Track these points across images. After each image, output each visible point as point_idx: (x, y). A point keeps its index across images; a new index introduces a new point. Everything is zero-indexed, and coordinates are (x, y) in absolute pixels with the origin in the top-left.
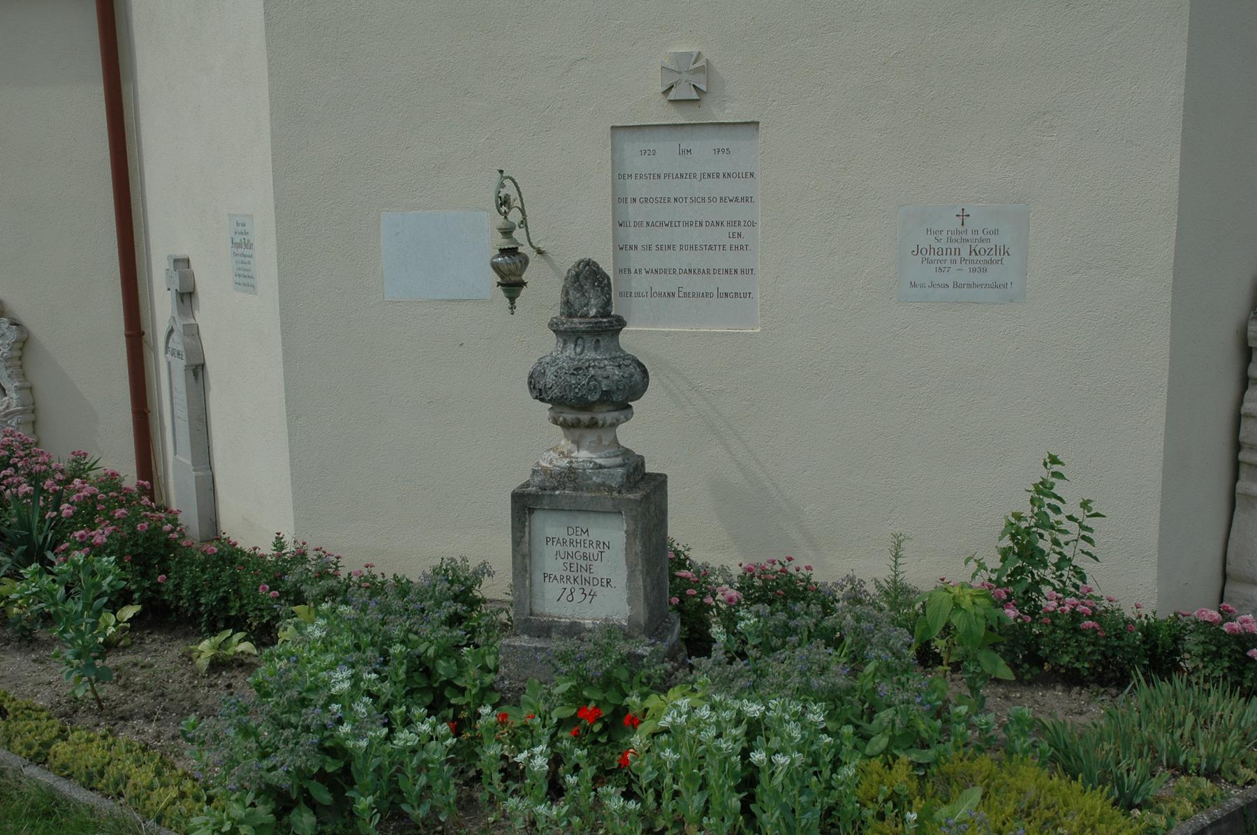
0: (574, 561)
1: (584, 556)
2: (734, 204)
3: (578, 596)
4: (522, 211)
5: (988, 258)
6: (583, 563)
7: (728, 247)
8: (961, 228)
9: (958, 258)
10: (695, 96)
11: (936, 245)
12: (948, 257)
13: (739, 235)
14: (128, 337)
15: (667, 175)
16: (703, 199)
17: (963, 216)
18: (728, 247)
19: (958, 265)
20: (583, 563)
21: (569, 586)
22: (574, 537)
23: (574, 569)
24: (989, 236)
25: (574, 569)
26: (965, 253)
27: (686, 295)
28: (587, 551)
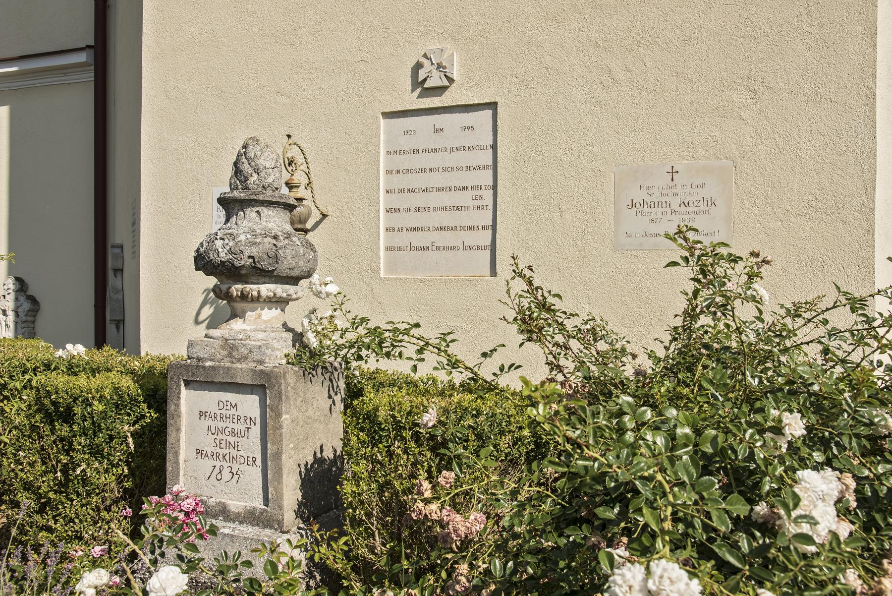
0: (224, 437)
1: (233, 433)
2: (477, 171)
3: (226, 475)
4: (308, 174)
5: (696, 209)
6: (231, 439)
7: (471, 208)
8: (670, 184)
9: (668, 210)
10: (445, 82)
11: (648, 199)
12: (660, 210)
13: (481, 197)
14: (96, 306)
15: (424, 150)
16: (452, 169)
17: (673, 172)
18: (471, 208)
19: (669, 217)
20: (231, 439)
21: (218, 464)
22: (223, 412)
23: (223, 446)
24: (696, 190)
25: (223, 446)
26: (675, 206)
27: (438, 248)
28: (235, 426)
